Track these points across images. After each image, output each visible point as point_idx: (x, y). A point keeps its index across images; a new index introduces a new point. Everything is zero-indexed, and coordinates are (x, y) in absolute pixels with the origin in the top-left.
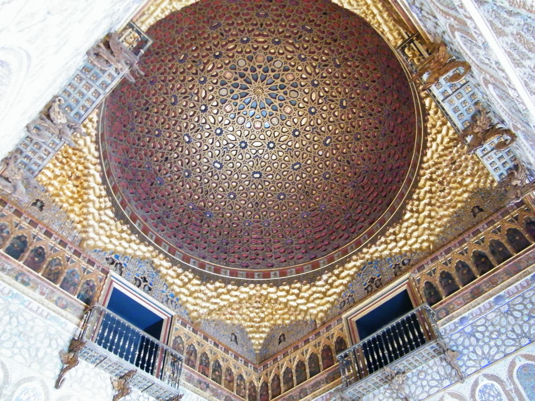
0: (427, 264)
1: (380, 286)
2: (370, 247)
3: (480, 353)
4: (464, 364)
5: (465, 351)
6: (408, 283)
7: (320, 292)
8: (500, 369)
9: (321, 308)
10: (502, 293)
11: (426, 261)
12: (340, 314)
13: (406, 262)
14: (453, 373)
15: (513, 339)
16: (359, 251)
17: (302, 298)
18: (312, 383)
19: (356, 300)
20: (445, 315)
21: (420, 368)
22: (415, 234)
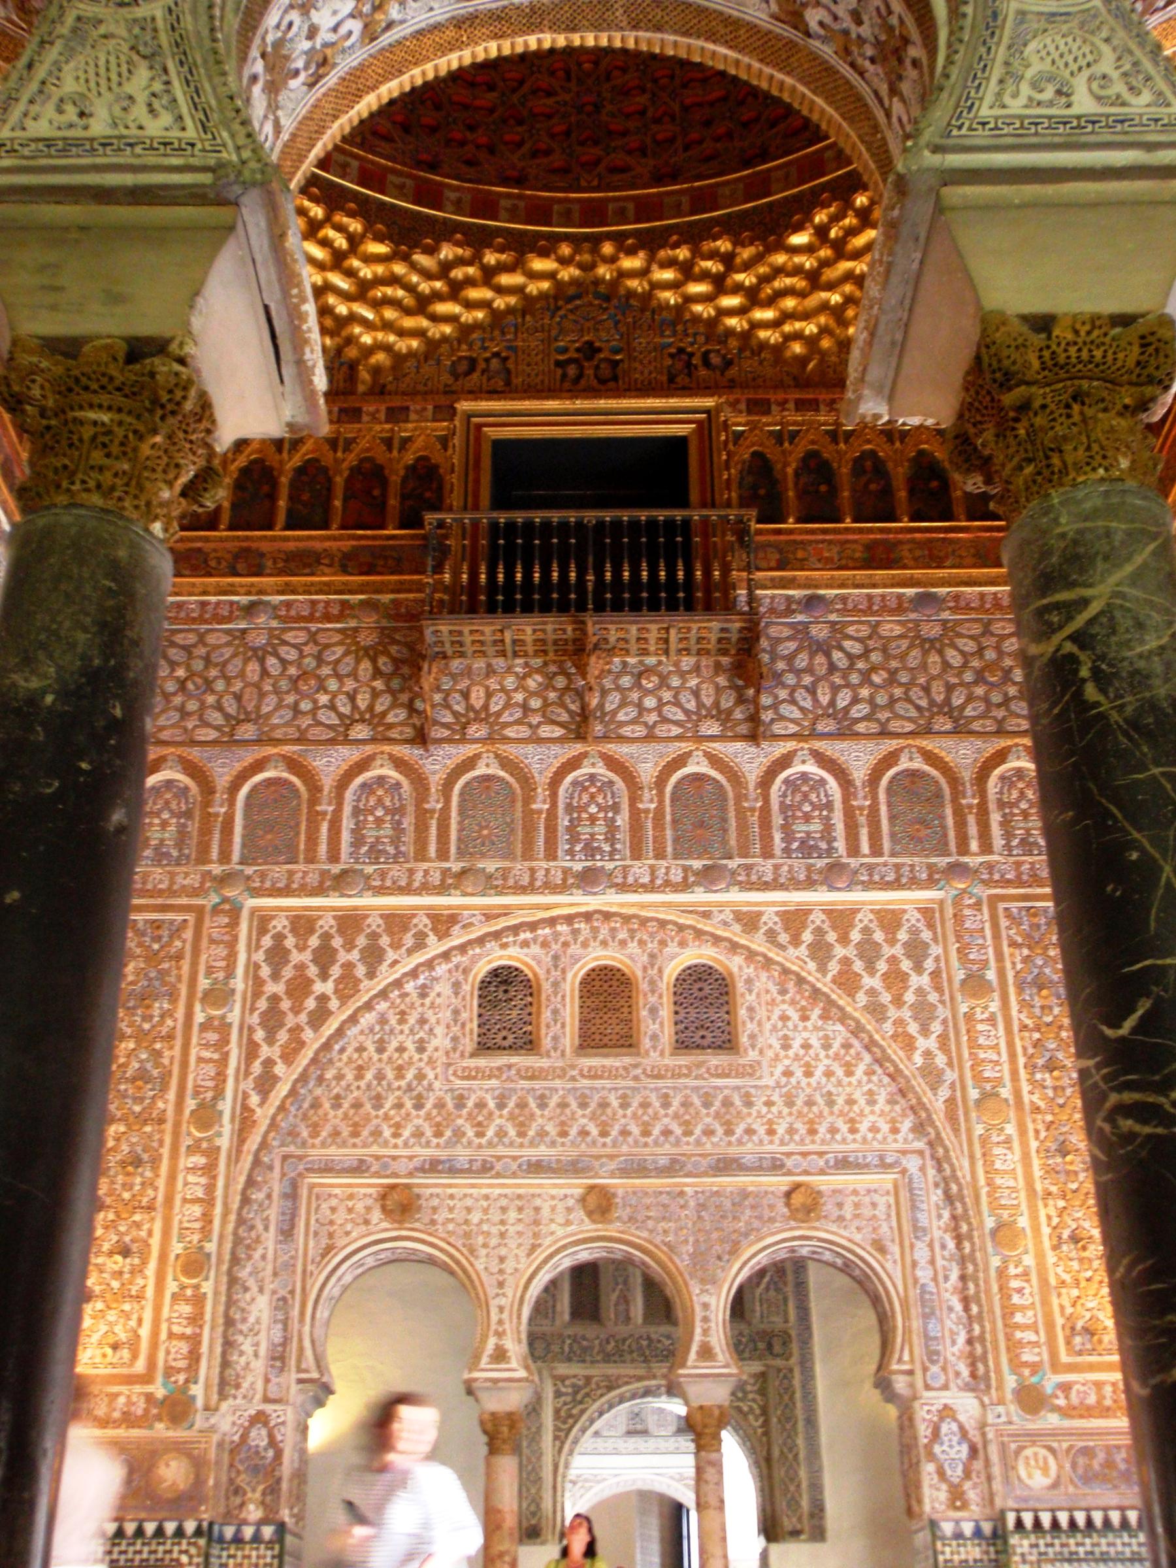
0: (783, 404)
1: (612, 381)
2: (631, 252)
3: (824, 700)
4: (775, 707)
5: (790, 679)
6: (699, 423)
7: (411, 289)
8: (859, 758)
9: (392, 338)
10: (942, 591)
11: (780, 396)
12: (454, 394)
13: (715, 360)
14: (738, 715)
15: (919, 708)
16: (587, 238)
17: (350, 273)
18: (291, 546)
19: (517, 381)
20: (773, 564)
21: (651, 661)
22: (790, 303)
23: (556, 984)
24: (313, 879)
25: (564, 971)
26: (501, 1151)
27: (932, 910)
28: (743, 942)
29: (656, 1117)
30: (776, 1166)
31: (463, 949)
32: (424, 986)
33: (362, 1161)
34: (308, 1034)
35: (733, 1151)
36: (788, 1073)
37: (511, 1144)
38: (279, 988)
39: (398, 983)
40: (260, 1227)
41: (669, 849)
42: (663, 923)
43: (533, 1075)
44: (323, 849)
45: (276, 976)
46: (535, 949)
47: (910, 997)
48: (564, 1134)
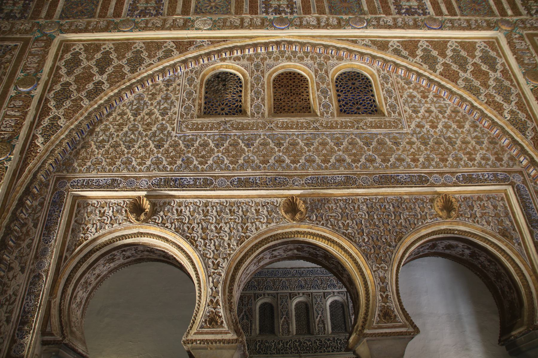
23: (258, 79)
24: (103, 23)
25: (263, 72)
26: (217, 173)
27: (493, 43)
28: (379, 55)
29: (332, 151)
30: (422, 181)
31: (196, 59)
32: (168, 81)
33: (114, 180)
34: (86, 103)
35: (390, 172)
36: (419, 126)
37: (227, 168)
38: (71, 79)
39: (152, 77)
40: (31, 225)
41: (327, 10)
42: (326, 47)
43: (243, 128)
44: (111, 11)
45: (69, 74)
46: (246, 62)
47: (492, 83)
48: (266, 162)
